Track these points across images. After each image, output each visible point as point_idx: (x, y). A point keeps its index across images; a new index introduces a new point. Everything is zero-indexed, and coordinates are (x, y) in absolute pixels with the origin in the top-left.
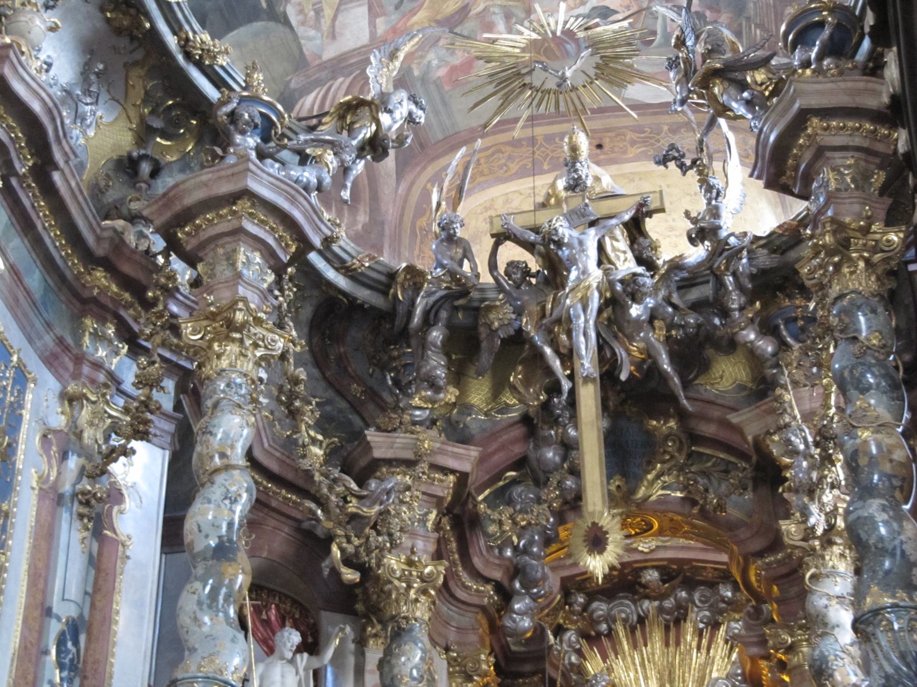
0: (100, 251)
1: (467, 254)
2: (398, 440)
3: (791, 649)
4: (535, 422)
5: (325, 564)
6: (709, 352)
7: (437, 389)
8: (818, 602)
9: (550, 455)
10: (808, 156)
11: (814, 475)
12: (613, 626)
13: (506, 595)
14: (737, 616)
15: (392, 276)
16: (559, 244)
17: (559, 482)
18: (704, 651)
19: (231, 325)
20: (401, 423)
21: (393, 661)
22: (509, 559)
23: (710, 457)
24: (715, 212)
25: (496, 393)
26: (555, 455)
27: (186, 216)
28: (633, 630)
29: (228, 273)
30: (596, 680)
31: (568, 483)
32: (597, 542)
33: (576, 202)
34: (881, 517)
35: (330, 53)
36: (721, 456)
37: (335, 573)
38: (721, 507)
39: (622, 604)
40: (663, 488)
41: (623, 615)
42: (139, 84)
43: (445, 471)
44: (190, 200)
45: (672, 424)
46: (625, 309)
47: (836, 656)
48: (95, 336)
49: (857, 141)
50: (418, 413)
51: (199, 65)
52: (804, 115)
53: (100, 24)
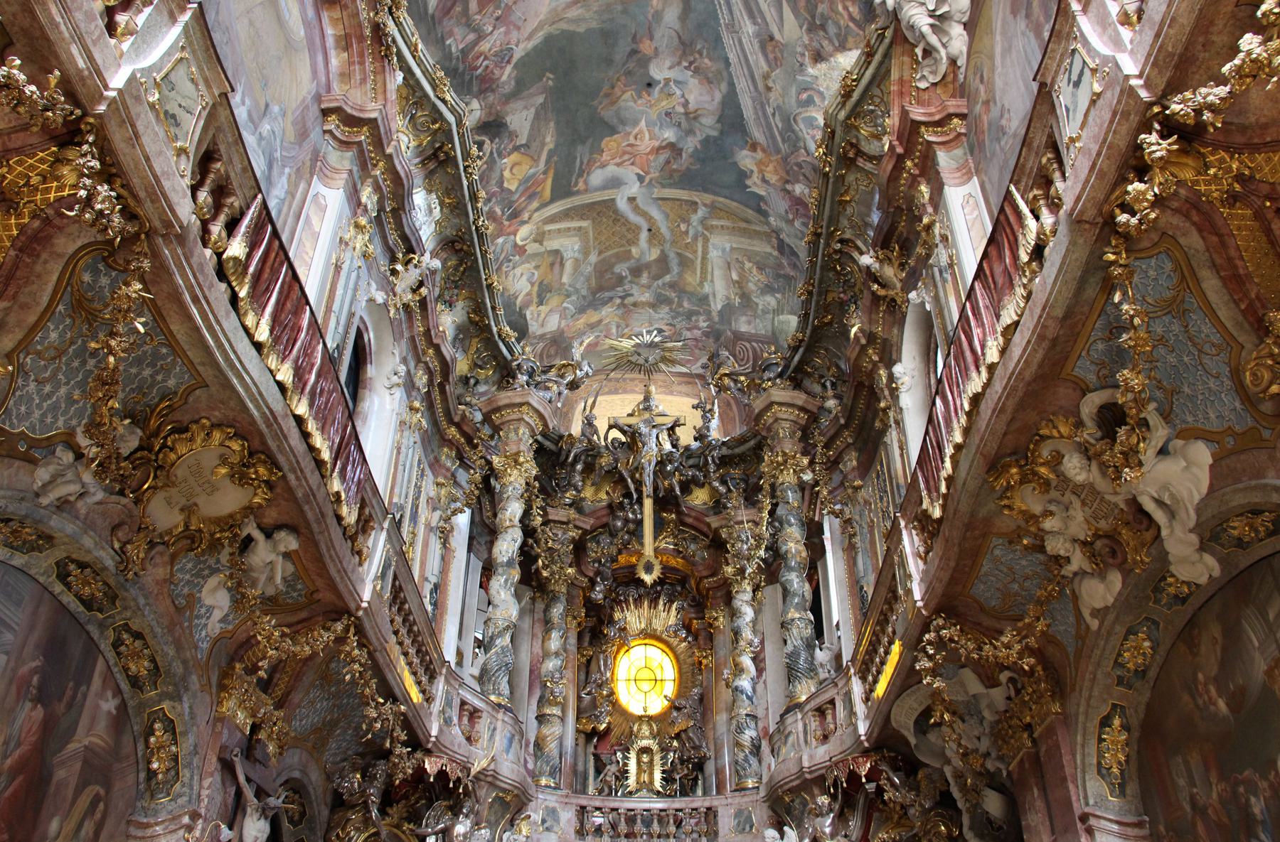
0: (457, 419)
1: (596, 432)
3: (716, 619)
5: (534, 567)
6: (692, 486)
7: (579, 491)
8: (737, 603)
9: (619, 524)
10: (771, 421)
13: (593, 582)
15: (561, 437)
16: (640, 434)
19: (516, 462)
24: (708, 429)
25: (597, 491)
27: (498, 409)
28: (635, 600)
29: (515, 438)
32: (649, 568)
33: (647, 415)
34: (796, 581)
35: (539, 332)
37: (537, 570)
38: (694, 556)
42: (475, 344)
43: (576, 527)
44: (501, 403)
46: (666, 466)
48: (447, 456)
49: (792, 417)
51: (503, 341)
52: (772, 404)
53: (465, 318)
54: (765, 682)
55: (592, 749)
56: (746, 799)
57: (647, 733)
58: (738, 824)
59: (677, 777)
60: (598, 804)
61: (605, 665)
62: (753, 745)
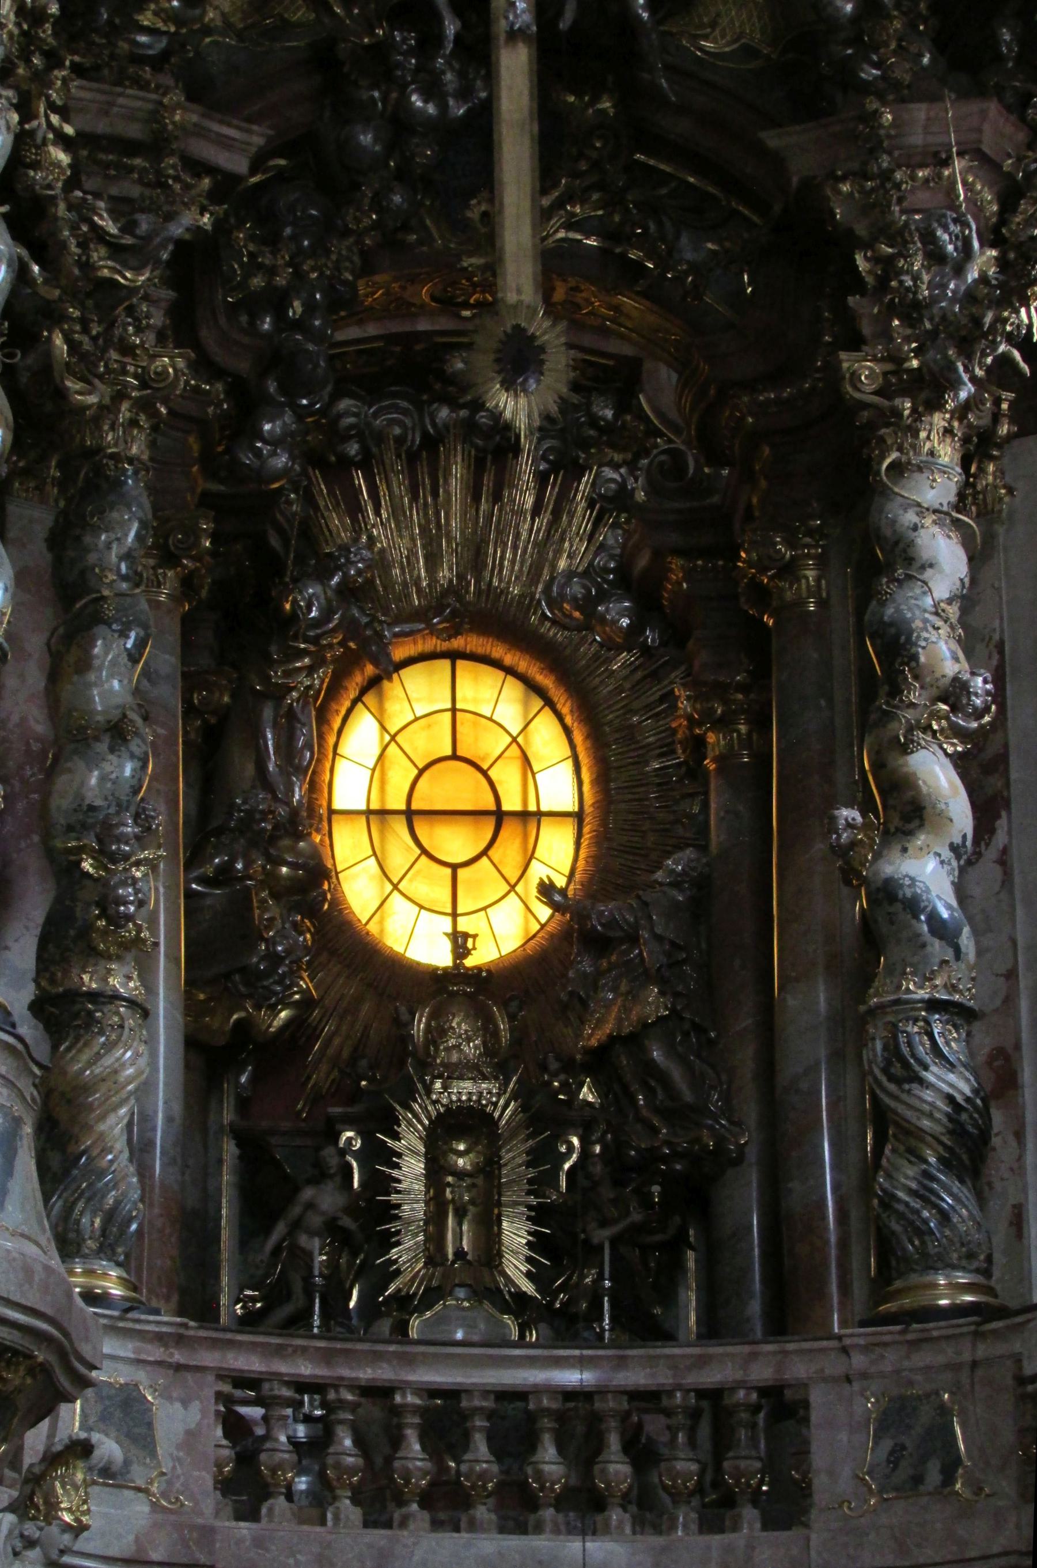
2: (121, 101)
3: (789, 570)
4: (346, 69)
9: (366, 139)
11: (988, 318)
12: (375, 450)
14: (618, 457)
17: (376, 194)
18: (546, 518)
20: (112, 56)
21: (88, 539)
22: (267, 336)
23: (665, 178)
26: (376, 140)
30: (348, 559)
31: (397, 199)
36: (692, 180)
39: (396, 409)
40: (569, 226)
41: (397, 431)
43: (197, 167)
45: (606, 105)
47: (925, 621)
50: (143, 39)
54: (1003, 860)
55: (228, 1116)
56: (924, 1358)
57: (471, 1050)
58: (895, 1457)
59: (602, 1235)
60: (306, 1369)
61: (288, 751)
62: (957, 1129)
